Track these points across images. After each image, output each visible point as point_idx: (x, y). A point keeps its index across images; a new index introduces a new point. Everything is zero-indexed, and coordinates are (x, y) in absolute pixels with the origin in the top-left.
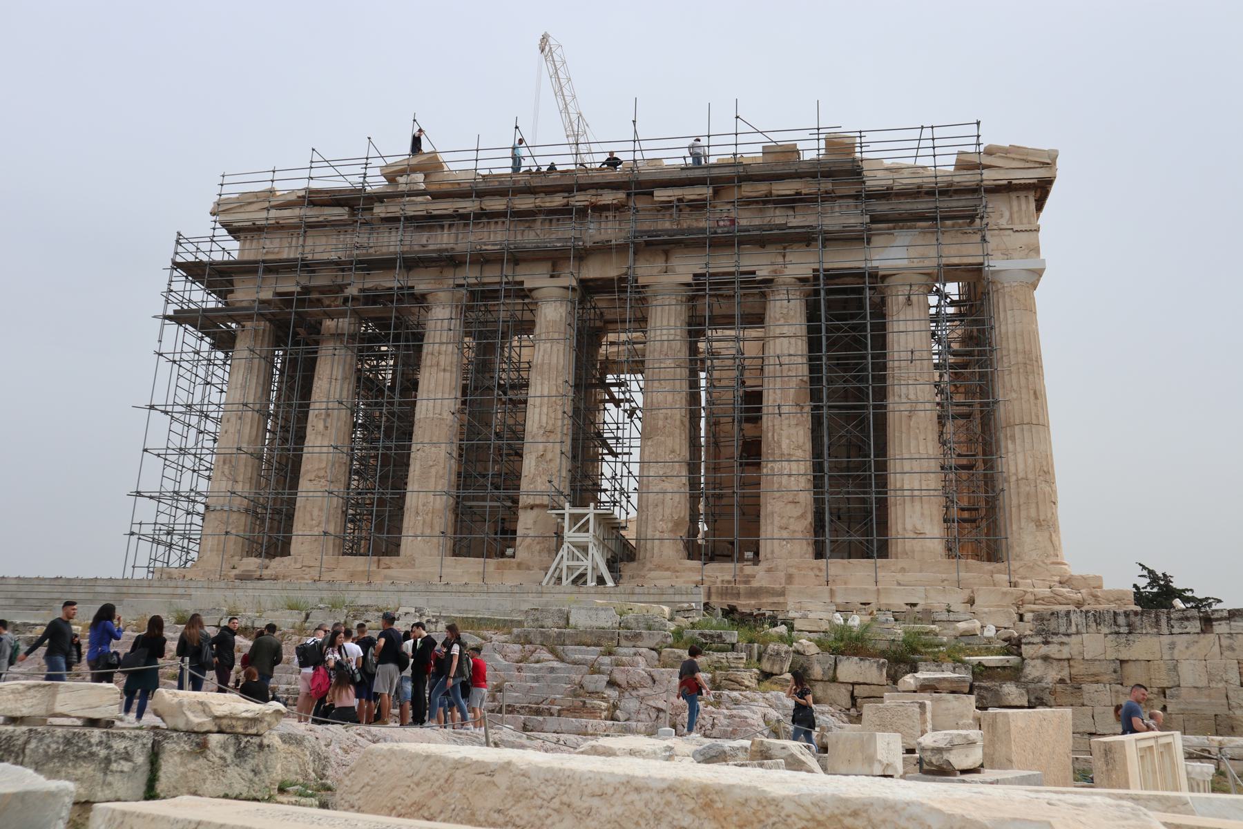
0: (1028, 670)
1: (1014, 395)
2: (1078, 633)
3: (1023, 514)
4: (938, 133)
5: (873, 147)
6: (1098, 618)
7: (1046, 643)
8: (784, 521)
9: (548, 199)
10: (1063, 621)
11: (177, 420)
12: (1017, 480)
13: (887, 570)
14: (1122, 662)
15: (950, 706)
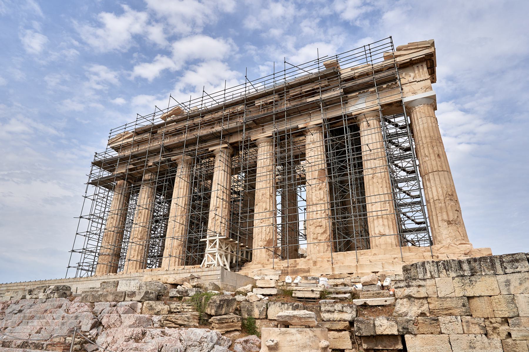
0: (397, 308)
1: (427, 159)
2: (432, 277)
3: (440, 218)
4: (371, 46)
5: (342, 60)
6: (447, 265)
7: (408, 286)
8: (315, 235)
9: (216, 114)
10: (420, 270)
11: (94, 222)
12: (434, 201)
13: (365, 256)
14: (469, 298)
15: (294, 338)
